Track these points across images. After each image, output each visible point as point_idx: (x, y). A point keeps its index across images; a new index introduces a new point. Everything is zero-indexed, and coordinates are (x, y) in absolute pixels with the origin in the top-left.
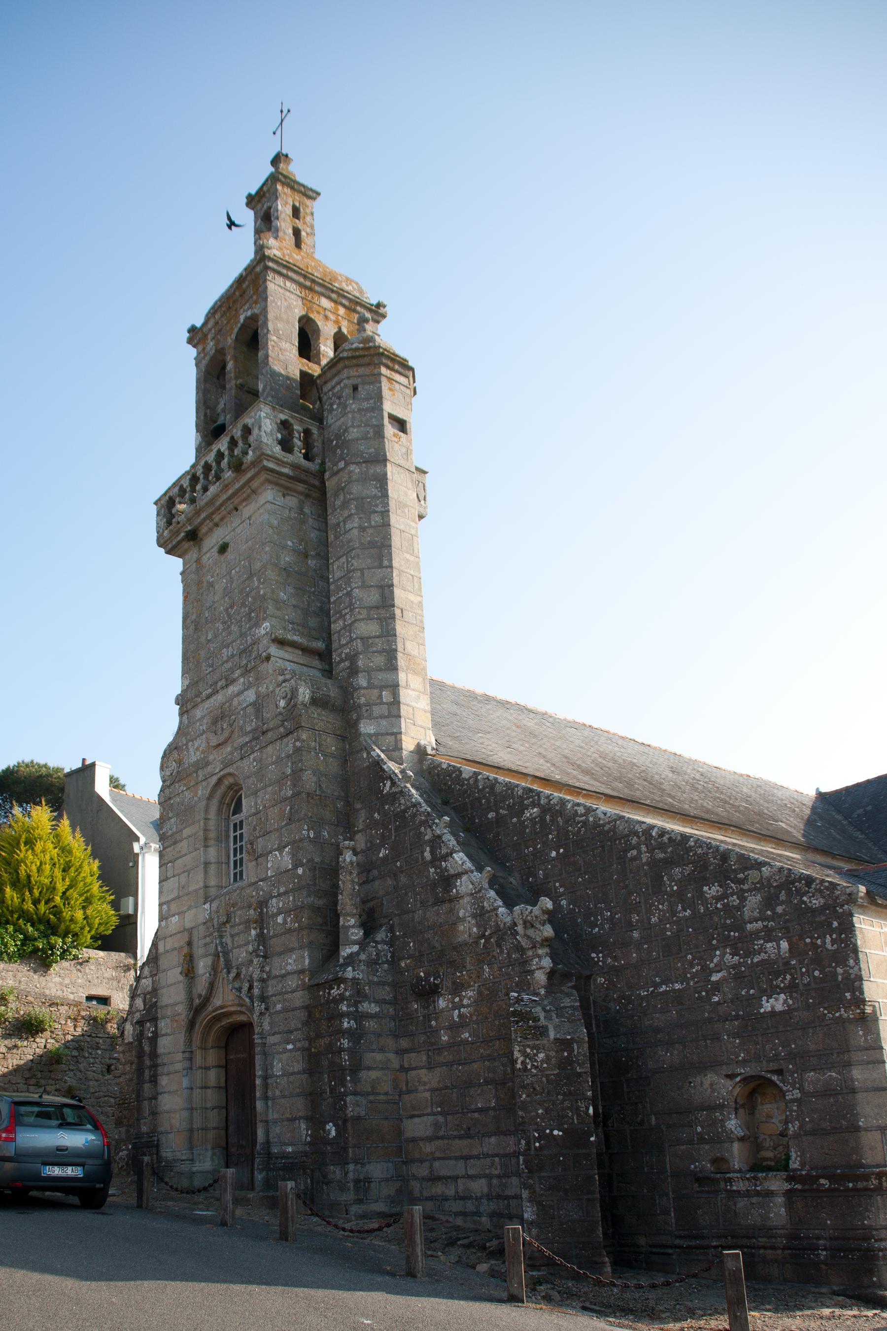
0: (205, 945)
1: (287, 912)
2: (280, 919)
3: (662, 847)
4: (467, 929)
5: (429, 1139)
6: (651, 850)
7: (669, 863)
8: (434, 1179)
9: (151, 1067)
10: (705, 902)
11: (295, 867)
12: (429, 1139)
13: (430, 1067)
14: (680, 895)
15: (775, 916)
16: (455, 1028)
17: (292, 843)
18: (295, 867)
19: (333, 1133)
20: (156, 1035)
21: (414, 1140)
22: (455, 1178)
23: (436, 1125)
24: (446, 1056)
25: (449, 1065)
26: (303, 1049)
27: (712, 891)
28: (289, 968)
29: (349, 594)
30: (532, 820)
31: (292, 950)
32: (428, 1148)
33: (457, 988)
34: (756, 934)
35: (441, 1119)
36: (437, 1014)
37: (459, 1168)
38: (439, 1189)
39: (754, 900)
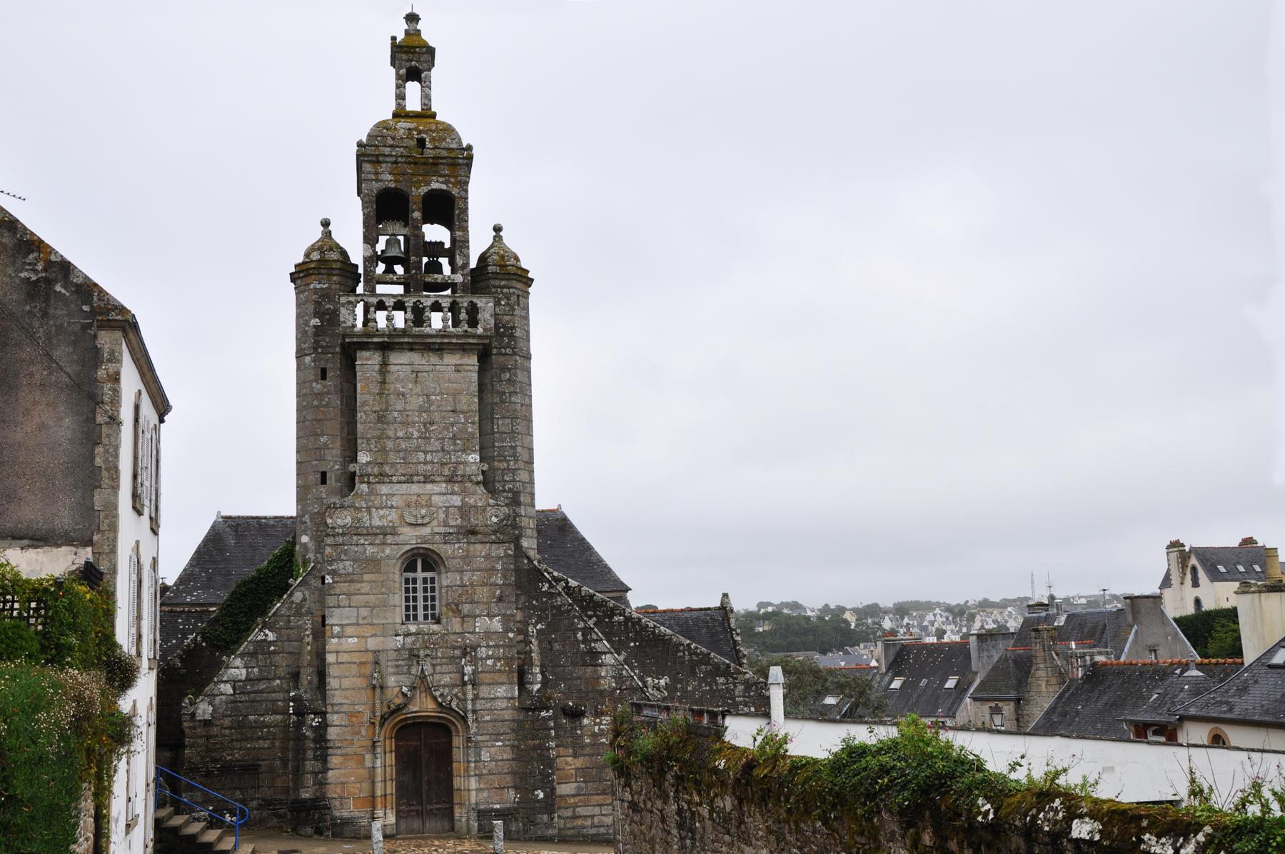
0: (397, 666)
1: (498, 659)
2: (490, 662)
3: (697, 655)
4: (608, 683)
5: (574, 796)
6: (690, 654)
7: (700, 663)
8: (575, 817)
9: (316, 749)
10: (717, 684)
11: (507, 631)
12: (574, 796)
13: (575, 756)
14: (703, 679)
15: (749, 697)
16: (594, 735)
17: (504, 615)
18: (507, 632)
19: (541, 795)
20: (324, 726)
21: (561, 796)
22: (592, 817)
23: (579, 788)
24: (587, 750)
25: (590, 755)
26: (513, 746)
27: (721, 680)
28: (499, 695)
29: (513, 448)
30: (619, 623)
31: (503, 684)
32: (572, 800)
33: (598, 714)
34: (740, 703)
35: (583, 785)
36: (582, 728)
37: (597, 810)
38: (579, 822)
39: (741, 688)
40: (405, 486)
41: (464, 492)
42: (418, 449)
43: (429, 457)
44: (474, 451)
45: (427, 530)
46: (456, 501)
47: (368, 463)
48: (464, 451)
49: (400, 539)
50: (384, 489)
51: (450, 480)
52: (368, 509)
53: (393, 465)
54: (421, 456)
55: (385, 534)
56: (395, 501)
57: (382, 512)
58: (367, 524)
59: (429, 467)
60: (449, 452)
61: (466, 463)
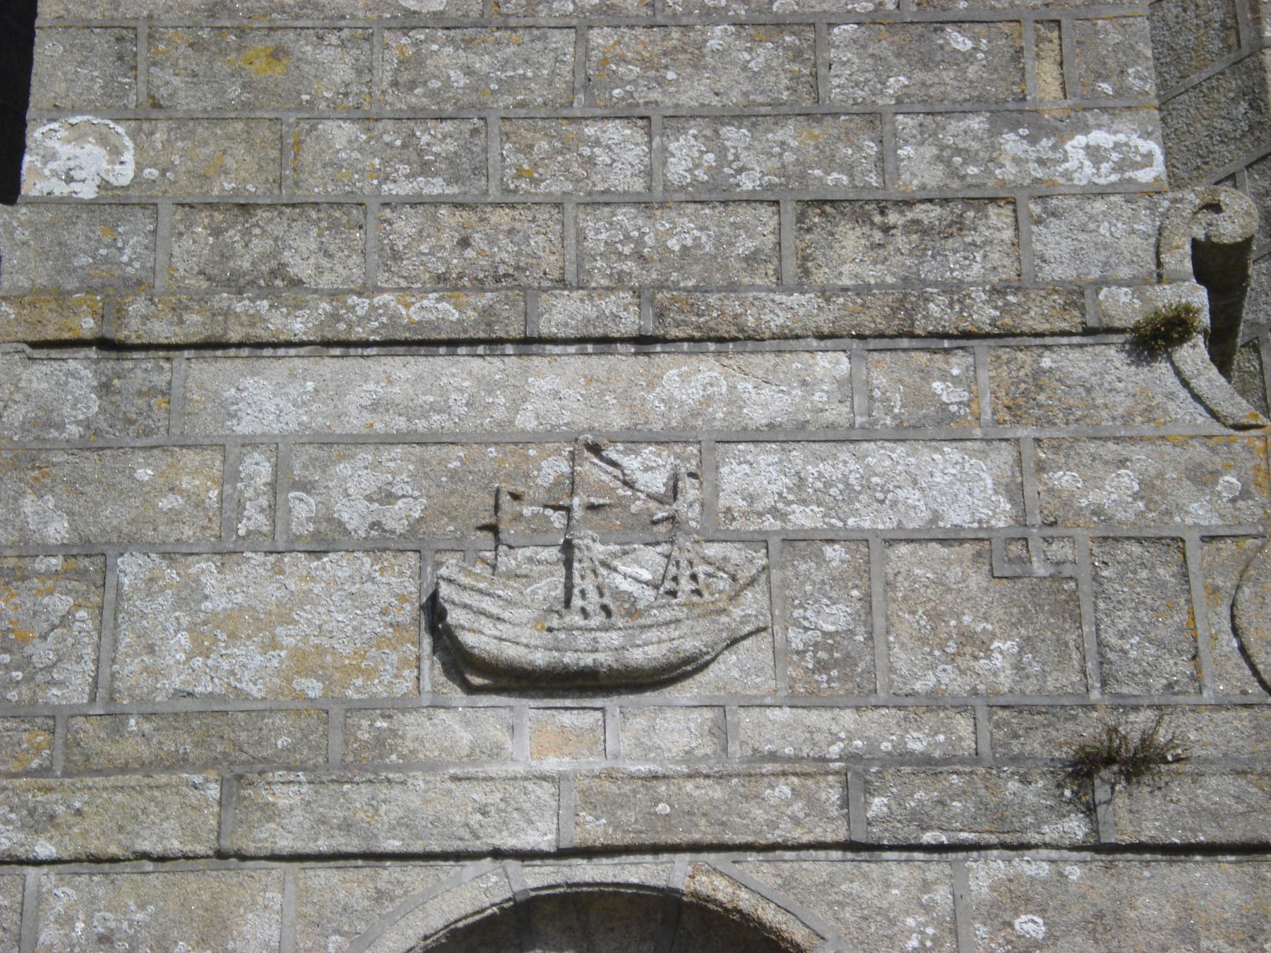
40: (459, 374)
41: (1028, 425)
42: (587, 99)
43: (685, 157)
44: (1118, 107)
45: (664, 730)
46: (963, 486)
47: (113, 203)
48: (1014, 112)
49: (391, 813)
50: (266, 399)
51: (896, 329)
52: (90, 560)
53: (346, 211)
54: (620, 152)
55: (239, 779)
56: (352, 492)
57: (220, 587)
58: (72, 688)
59: (683, 230)
60: (872, 117)
61: (1031, 202)
